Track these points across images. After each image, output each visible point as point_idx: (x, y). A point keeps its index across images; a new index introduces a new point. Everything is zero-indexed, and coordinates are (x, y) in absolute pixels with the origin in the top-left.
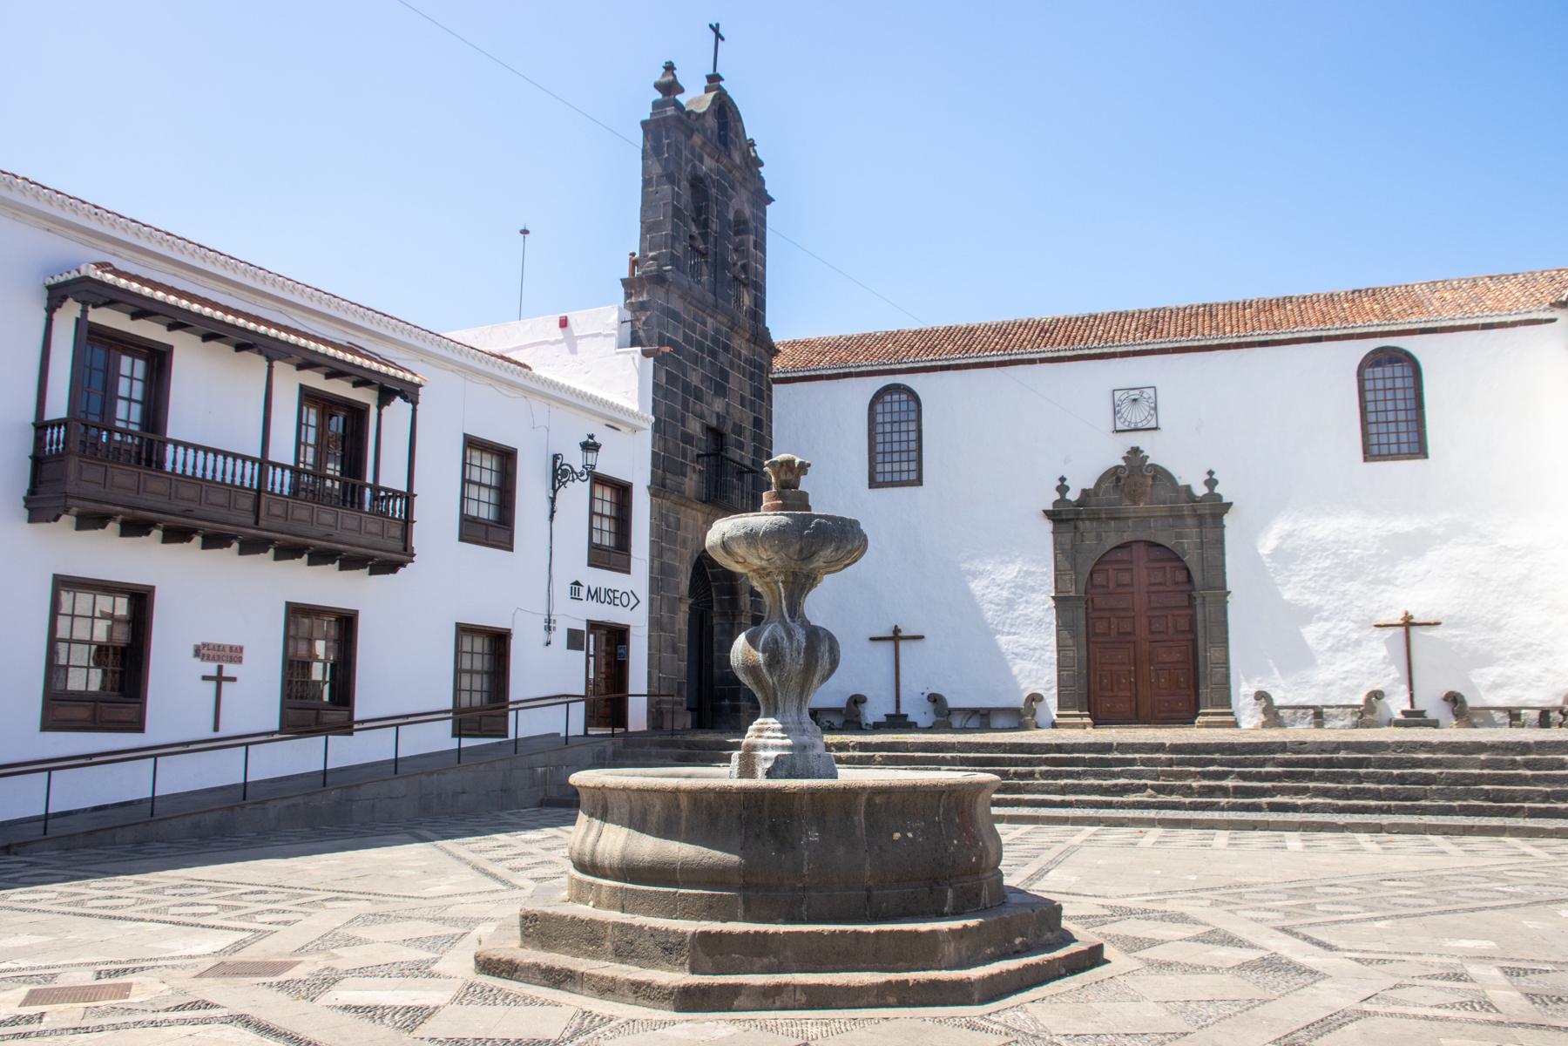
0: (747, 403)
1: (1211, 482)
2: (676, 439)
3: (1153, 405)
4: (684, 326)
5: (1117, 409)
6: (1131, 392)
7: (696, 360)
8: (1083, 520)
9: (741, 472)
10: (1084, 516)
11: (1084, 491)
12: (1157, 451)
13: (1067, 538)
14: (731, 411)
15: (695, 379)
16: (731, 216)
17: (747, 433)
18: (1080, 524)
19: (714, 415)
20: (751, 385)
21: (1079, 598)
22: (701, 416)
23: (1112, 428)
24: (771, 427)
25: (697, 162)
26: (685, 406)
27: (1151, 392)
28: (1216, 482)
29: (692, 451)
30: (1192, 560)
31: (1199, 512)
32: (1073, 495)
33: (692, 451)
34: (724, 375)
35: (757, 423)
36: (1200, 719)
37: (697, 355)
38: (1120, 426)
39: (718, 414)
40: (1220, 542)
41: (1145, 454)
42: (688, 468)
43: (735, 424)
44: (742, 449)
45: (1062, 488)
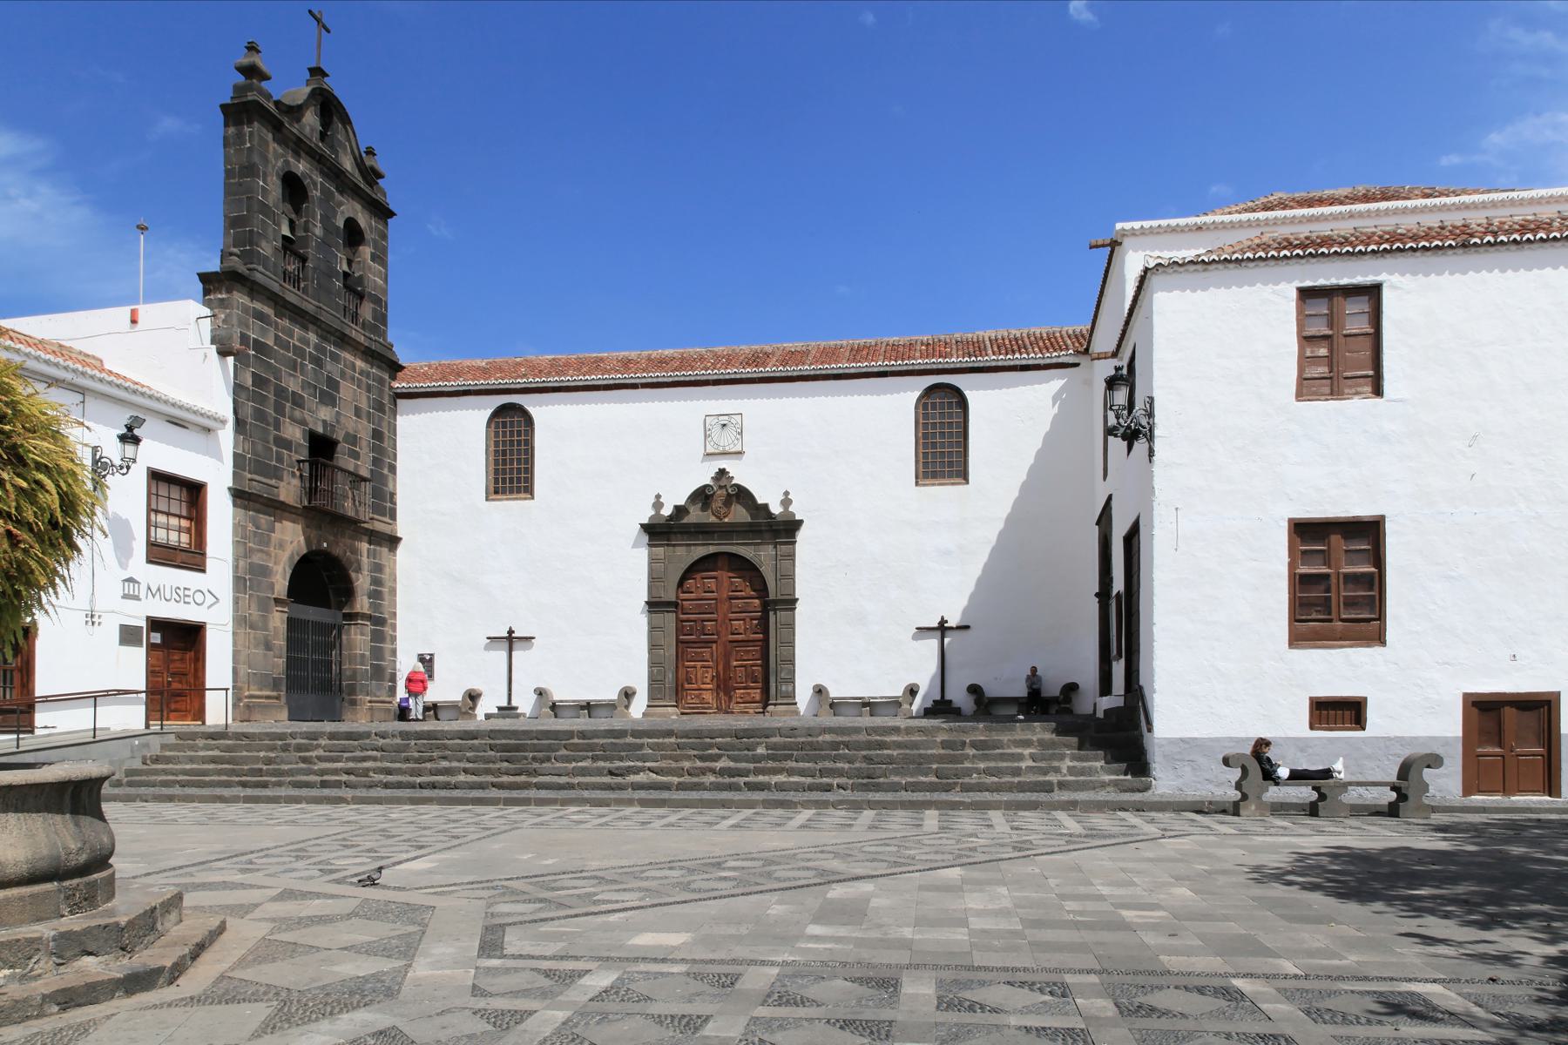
0: (364, 415)
2: (268, 442)
4: (277, 328)
7: (294, 366)
9: (357, 479)
14: (343, 420)
15: (293, 385)
16: (340, 223)
17: (364, 443)
19: (320, 423)
20: (369, 398)
22: (303, 422)
24: (395, 441)
25: (291, 160)
26: (280, 409)
29: (290, 456)
30: (767, 571)
33: (290, 456)
34: (333, 384)
35: (377, 435)
37: (295, 361)
39: (324, 422)
40: (791, 556)
42: (285, 472)
43: (347, 434)
44: (356, 456)
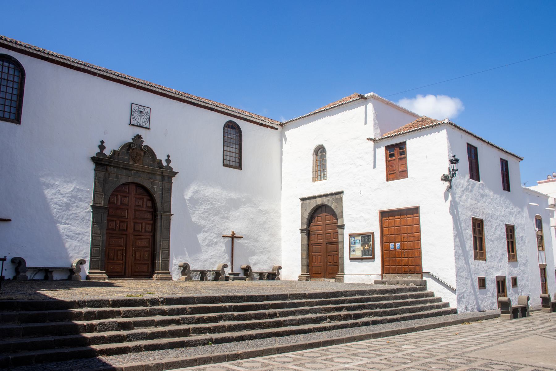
1: (168, 161)
3: (148, 117)
5: (133, 113)
6: (140, 107)
8: (111, 166)
10: (112, 164)
11: (114, 151)
12: (148, 140)
13: (101, 175)
18: (109, 168)
21: (105, 208)
23: (129, 122)
27: (148, 110)
28: (170, 161)
31: (164, 174)
32: (107, 152)
36: (155, 276)
38: (133, 122)
41: (143, 140)
45: (102, 147)
